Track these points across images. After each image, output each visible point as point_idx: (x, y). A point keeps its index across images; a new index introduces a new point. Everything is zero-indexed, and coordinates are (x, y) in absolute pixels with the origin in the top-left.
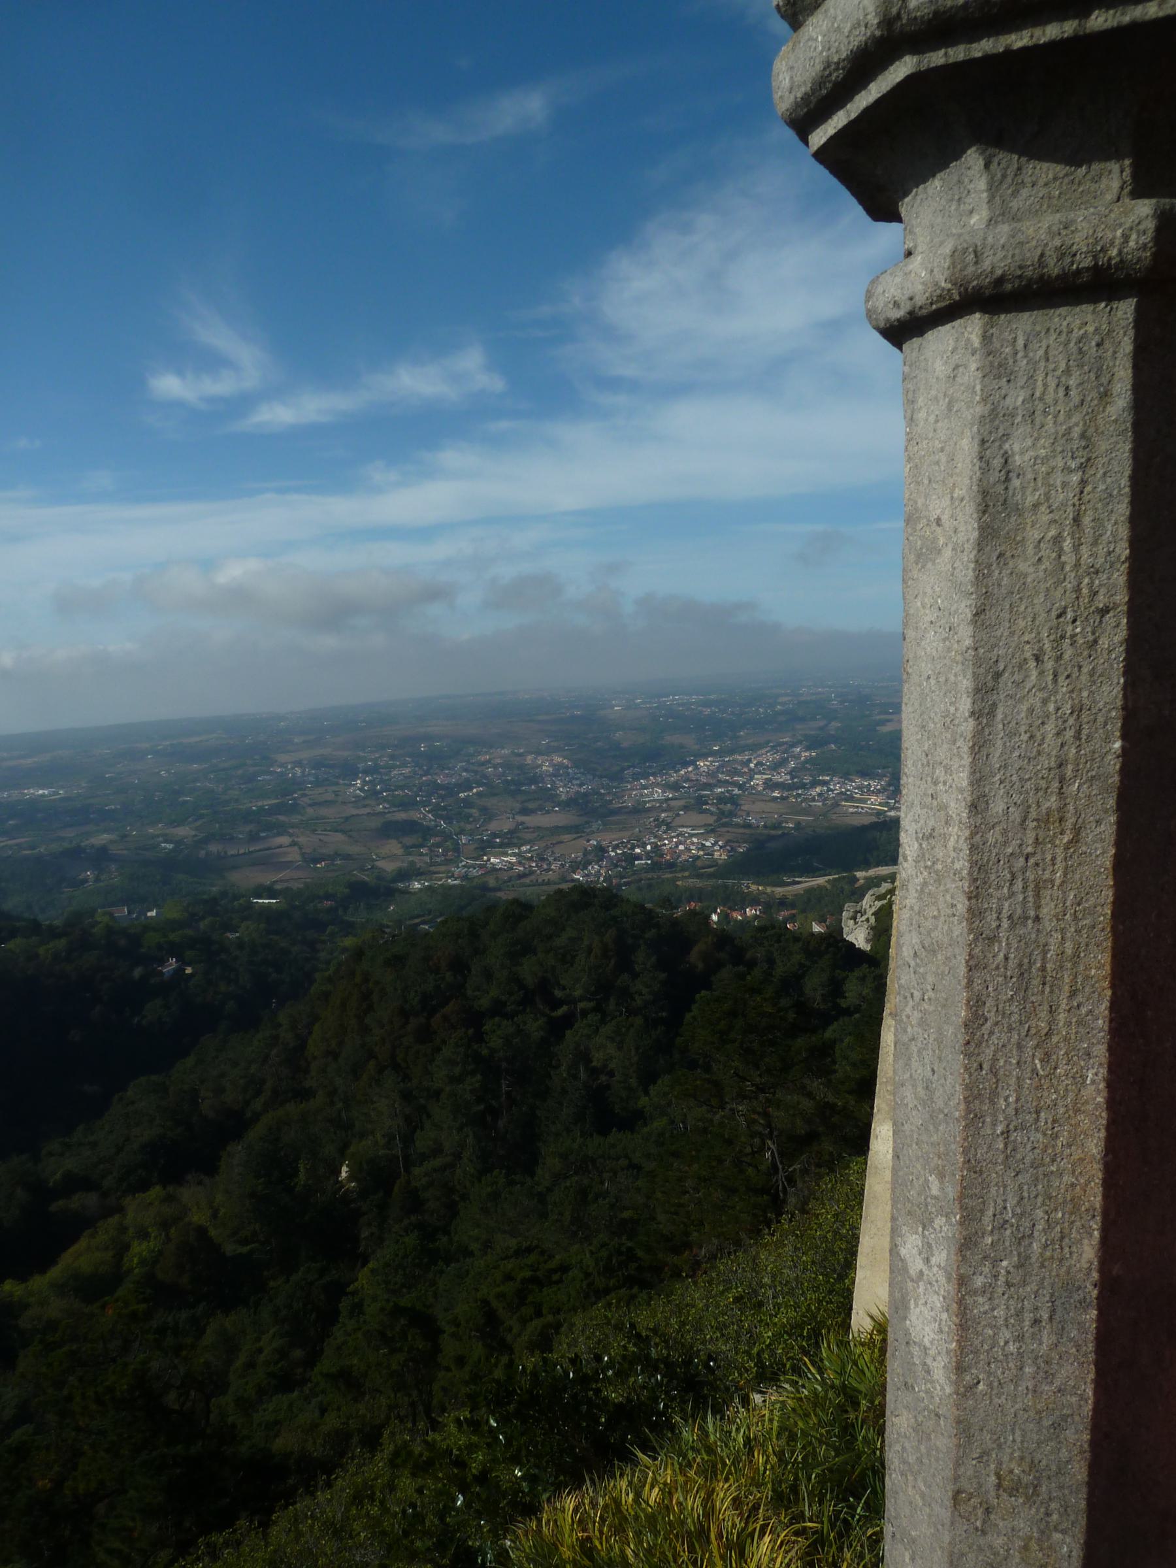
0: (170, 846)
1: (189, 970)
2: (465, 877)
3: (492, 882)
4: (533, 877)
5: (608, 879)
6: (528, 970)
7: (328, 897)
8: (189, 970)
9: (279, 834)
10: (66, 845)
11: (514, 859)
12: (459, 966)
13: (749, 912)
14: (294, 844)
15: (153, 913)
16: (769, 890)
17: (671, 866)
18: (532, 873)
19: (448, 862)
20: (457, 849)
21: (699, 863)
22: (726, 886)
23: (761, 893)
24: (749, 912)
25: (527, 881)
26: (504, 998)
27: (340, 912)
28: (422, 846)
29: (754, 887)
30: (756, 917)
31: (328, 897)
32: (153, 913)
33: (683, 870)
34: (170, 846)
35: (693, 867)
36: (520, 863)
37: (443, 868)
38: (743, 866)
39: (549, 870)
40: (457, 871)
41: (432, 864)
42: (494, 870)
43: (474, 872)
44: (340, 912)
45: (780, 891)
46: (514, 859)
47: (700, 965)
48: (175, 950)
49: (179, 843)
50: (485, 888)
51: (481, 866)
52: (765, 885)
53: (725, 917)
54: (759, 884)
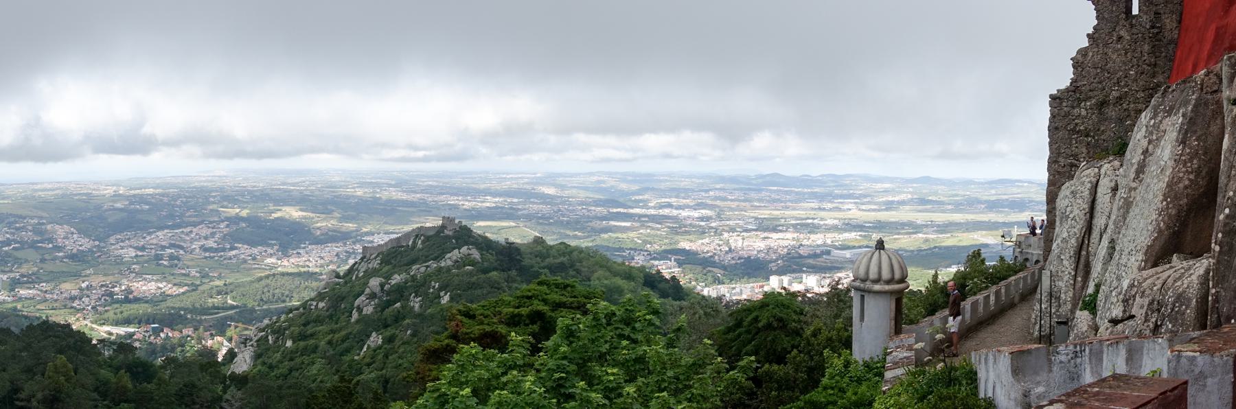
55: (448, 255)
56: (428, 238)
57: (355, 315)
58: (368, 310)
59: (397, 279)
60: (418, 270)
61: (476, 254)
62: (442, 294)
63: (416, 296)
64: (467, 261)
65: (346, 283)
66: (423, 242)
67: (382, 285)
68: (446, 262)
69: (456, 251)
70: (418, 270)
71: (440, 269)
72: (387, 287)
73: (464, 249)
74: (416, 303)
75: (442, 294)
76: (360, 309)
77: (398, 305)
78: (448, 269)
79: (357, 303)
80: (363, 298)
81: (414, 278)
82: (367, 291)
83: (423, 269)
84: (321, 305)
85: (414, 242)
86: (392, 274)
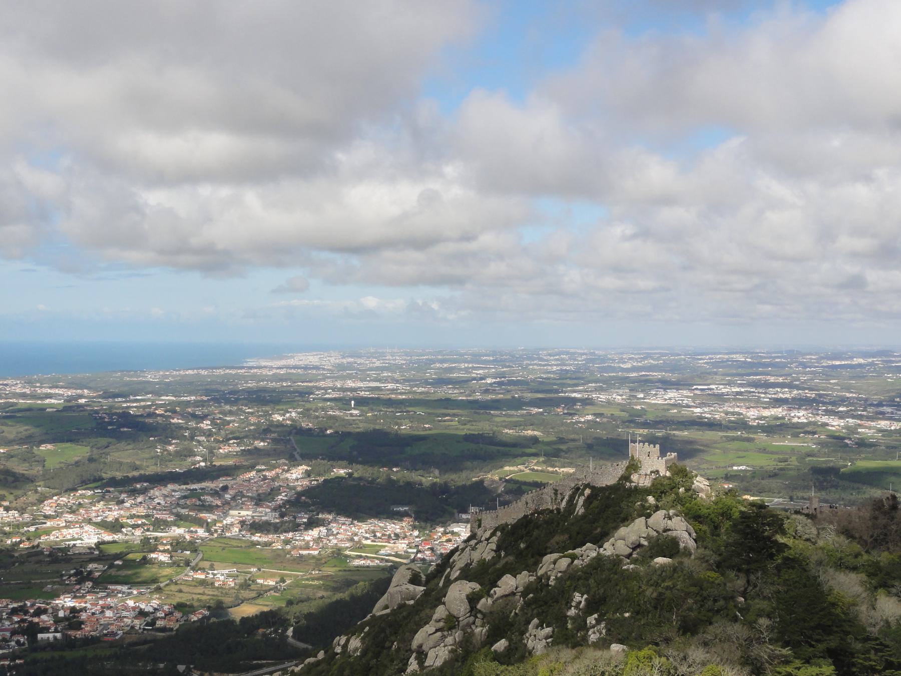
55: (622, 531)
56: (597, 492)
61: (681, 530)
63: (540, 626)
64: (666, 545)
65: (426, 594)
66: (589, 501)
67: (473, 599)
69: (640, 522)
70: (554, 565)
72: (484, 603)
75: (591, 620)
76: (422, 656)
78: (616, 561)
79: (419, 638)
80: (429, 628)
81: (540, 585)
82: (440, 612)
83: (564, 563)
84: (355, 643)
85: (571, 503)
86: (500, 577)
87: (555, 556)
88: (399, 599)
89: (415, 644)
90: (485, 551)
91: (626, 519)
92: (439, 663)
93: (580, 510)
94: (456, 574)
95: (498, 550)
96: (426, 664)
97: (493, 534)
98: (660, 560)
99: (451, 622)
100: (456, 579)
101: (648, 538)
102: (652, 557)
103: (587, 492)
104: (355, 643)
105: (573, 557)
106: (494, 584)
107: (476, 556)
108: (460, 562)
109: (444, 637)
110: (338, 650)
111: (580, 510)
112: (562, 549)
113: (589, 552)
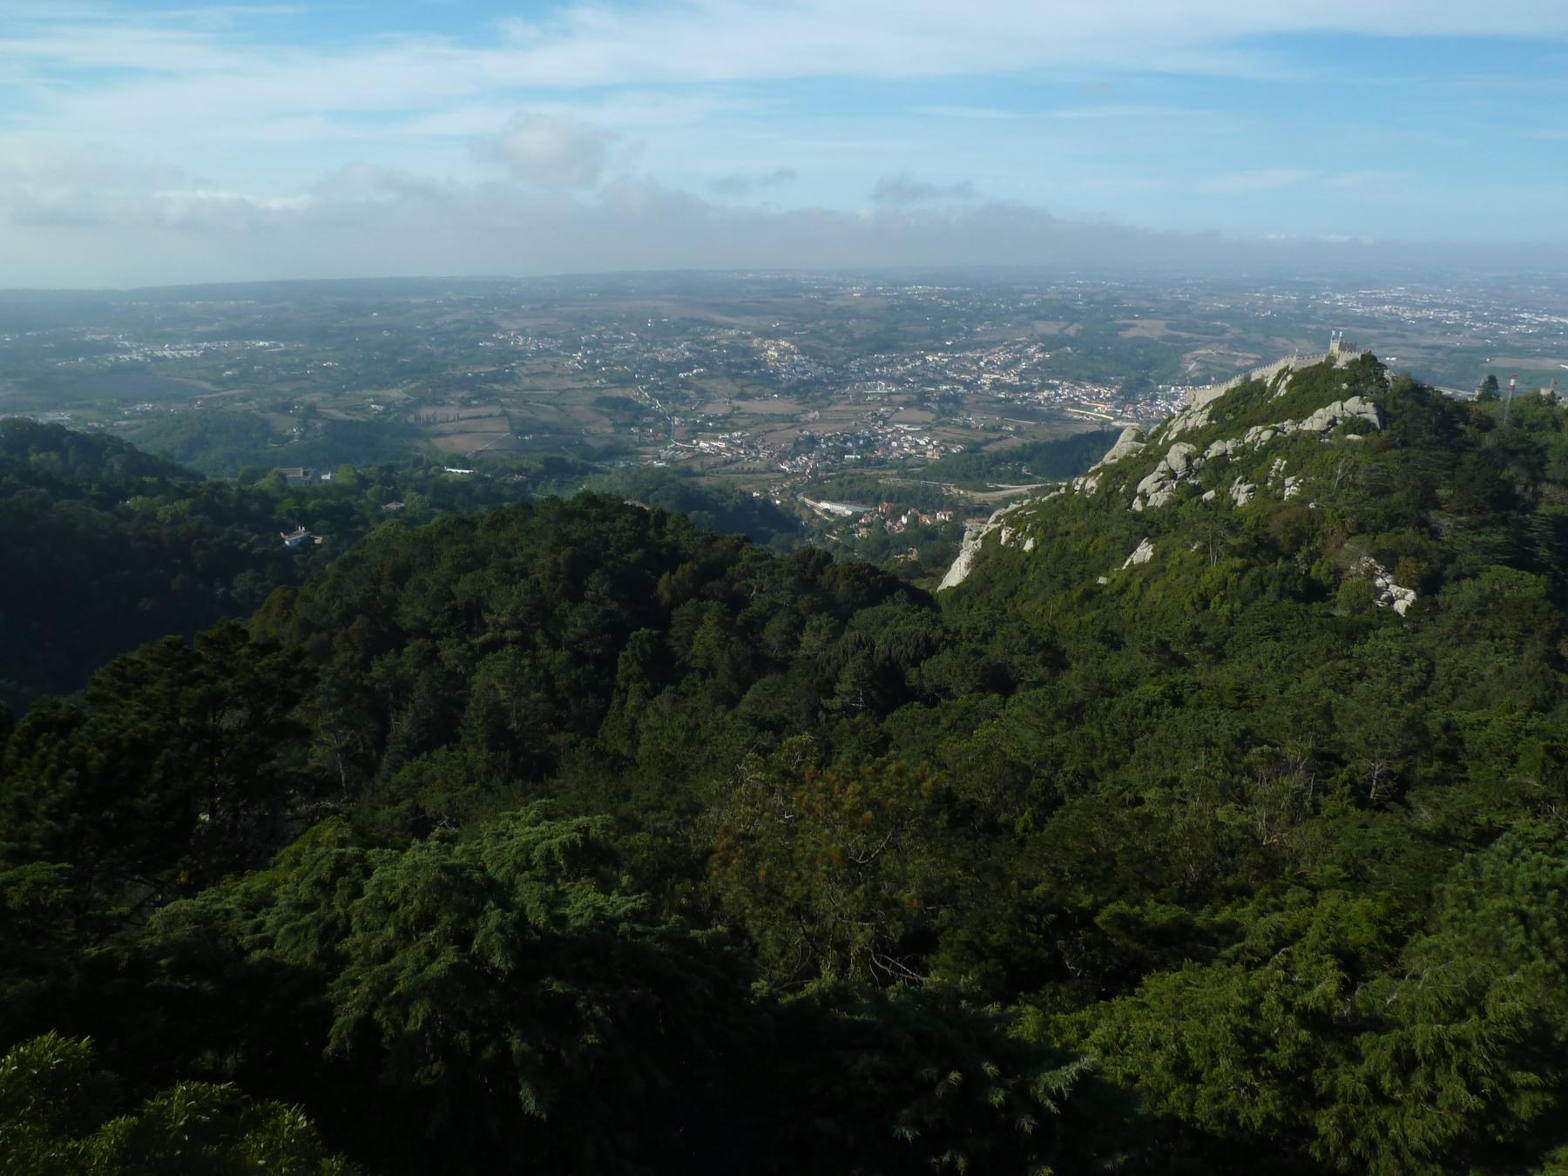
0: (380, 408)
1: (318, 540)
2: (671, 460)
3: (696, 466)
4: (739, 465)
5: (814, 472)
6: (465, 587)
7: (520, 471)
8: (318, 540)
9: (490, 403)
10: (280, 399)
11: (723, 445)
12: (401, 575)
13: (940, 516)
14: (504, 414)
15: (328, 477)
16: (970, 494)
17: (881, 463)
18: (739, 460)
19: (657, 443)
20: (668, 431)
21: (909, 462)
22: (926, 488)
23: (962, 497)
24: (940, 516)
25: (732, 467)
26: (427, 618)
27: (530, 487)
28: (633, 425)
29: (955, 491)
30: (944, 522)
31: (520, 471)
32: (328, 477)
33: (892, 468)
34: (380, 408)
35: (904, 466)
36: (728, 449)
37: (650, 449)
38: (948, 469)
39: (755, 459)
40: (663, 453)
41: (641, 444)
42: (702, 454)
43: (681, 455)
44: (530, 487)
45: (980, 497)
46: (723, 445)
47: (667, 596)
48: (306, 519)
49: (389, 405)
50: (688, 472)
51: (689, 450)
52: (965, 488)
53: (915, 520)
54: (960, 488)
55: (1320, 412)
57: (1137, 505)
58: (1158, 499)
59: (1216, 449)
60: (1259, 435)
62: (1288, 481)
65: (1147, 449)
66: (1289, 386)
67: (1189, 459)
68: (1315, 422)
69: (1338, 404)
70: (1259, 435)
71: (1295, 437)
73: (1353, 404)
74: (1241, 494)
75: (1288, 481)
76: (1145, 497)
77: (1209, 495)
82: (1162, 466)
84: (1091, 483)
87: (1260, 428)
88: (1124, 452)
89: (1140, 489)
90: (1200, 421)
91: (1323, 403)
92: (1159, 504)
93: (1282, 392)
94: (1172, 436)
95: (1210, 419)
96: (1150, 504)
97: (1207, 406)
98: (1350, 436)
99: (1172, 474)
100: (1175, 441)
101: (1343, 418)
102: (1345, 433)
103: (1290, 378)
104: (1091, 483)
105: (1276, 430)
106: (1207, 446)
107: (1190, 423)
108: (1177, 426)
109: (1163, 486)
110: (1078, 488)
111: (1282, 392)
112: (1264, 421)
113: (1289, 426)
